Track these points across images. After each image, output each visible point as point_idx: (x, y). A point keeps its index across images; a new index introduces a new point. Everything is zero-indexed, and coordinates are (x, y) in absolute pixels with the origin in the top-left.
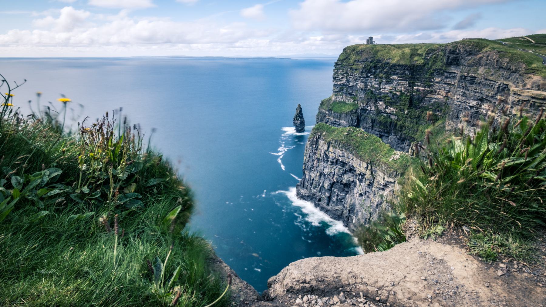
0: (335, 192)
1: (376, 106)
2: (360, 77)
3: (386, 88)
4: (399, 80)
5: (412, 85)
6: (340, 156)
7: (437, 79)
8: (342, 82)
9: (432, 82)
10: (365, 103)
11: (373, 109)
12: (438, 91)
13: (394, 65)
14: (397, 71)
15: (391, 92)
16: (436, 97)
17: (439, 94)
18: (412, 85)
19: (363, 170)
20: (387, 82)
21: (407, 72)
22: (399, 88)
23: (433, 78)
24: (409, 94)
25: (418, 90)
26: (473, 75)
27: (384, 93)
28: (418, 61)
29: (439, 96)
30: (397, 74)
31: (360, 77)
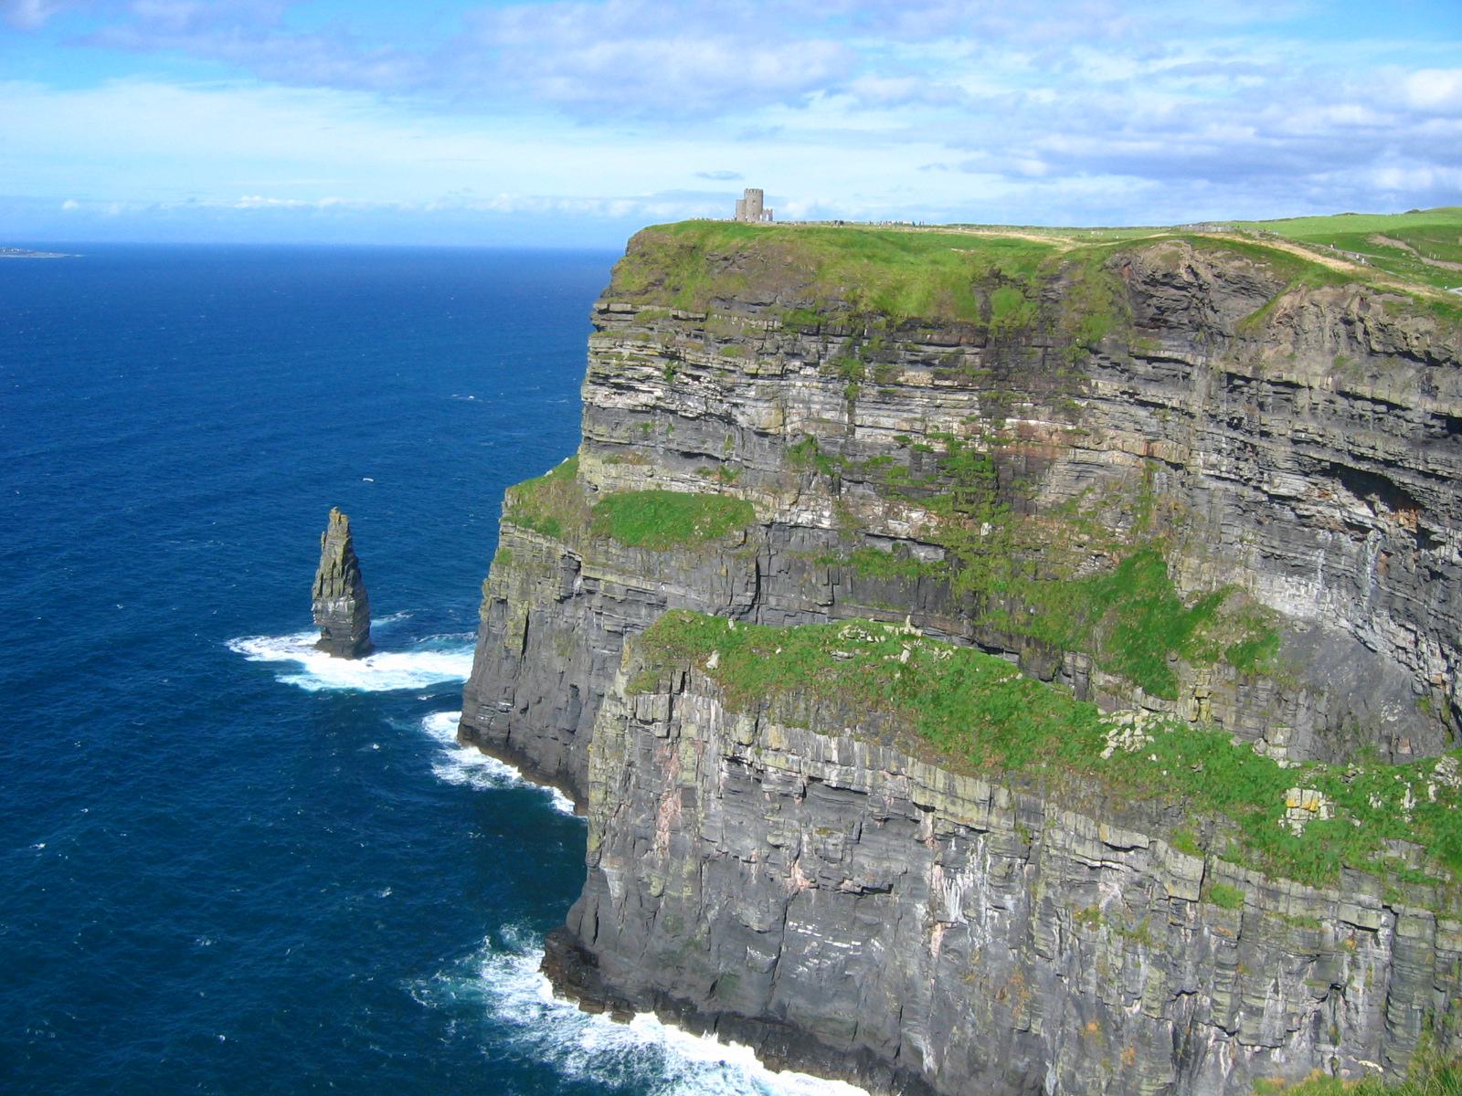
0: (805, 940)
1: (841, 511)
2: (754, 376)
3: (879, 427)
4: (936, 388)
5: (996, 410)
6: (828, 762)
7: (1106, 386)
8: (643, 398)
9: (1081, 396)
10: (788, 498)
11: (826, 524)
12: (1112, 433)
13: (911, 325)
14: (931, 350)
16: (1103, 458)
17: (1114, 448)
18: (996, 410)
19: (976, 816)
20: (885, 398)
21: (972, 357)
22: (940, 419)
23: (1087, 382)
24: (982, 449)
25: (1024, 434)
26: (1286, 377)
27: (872, 447)
28: (1008, 308)
29: (1116, 457)
30: (927, 363)
31: (754, 376)
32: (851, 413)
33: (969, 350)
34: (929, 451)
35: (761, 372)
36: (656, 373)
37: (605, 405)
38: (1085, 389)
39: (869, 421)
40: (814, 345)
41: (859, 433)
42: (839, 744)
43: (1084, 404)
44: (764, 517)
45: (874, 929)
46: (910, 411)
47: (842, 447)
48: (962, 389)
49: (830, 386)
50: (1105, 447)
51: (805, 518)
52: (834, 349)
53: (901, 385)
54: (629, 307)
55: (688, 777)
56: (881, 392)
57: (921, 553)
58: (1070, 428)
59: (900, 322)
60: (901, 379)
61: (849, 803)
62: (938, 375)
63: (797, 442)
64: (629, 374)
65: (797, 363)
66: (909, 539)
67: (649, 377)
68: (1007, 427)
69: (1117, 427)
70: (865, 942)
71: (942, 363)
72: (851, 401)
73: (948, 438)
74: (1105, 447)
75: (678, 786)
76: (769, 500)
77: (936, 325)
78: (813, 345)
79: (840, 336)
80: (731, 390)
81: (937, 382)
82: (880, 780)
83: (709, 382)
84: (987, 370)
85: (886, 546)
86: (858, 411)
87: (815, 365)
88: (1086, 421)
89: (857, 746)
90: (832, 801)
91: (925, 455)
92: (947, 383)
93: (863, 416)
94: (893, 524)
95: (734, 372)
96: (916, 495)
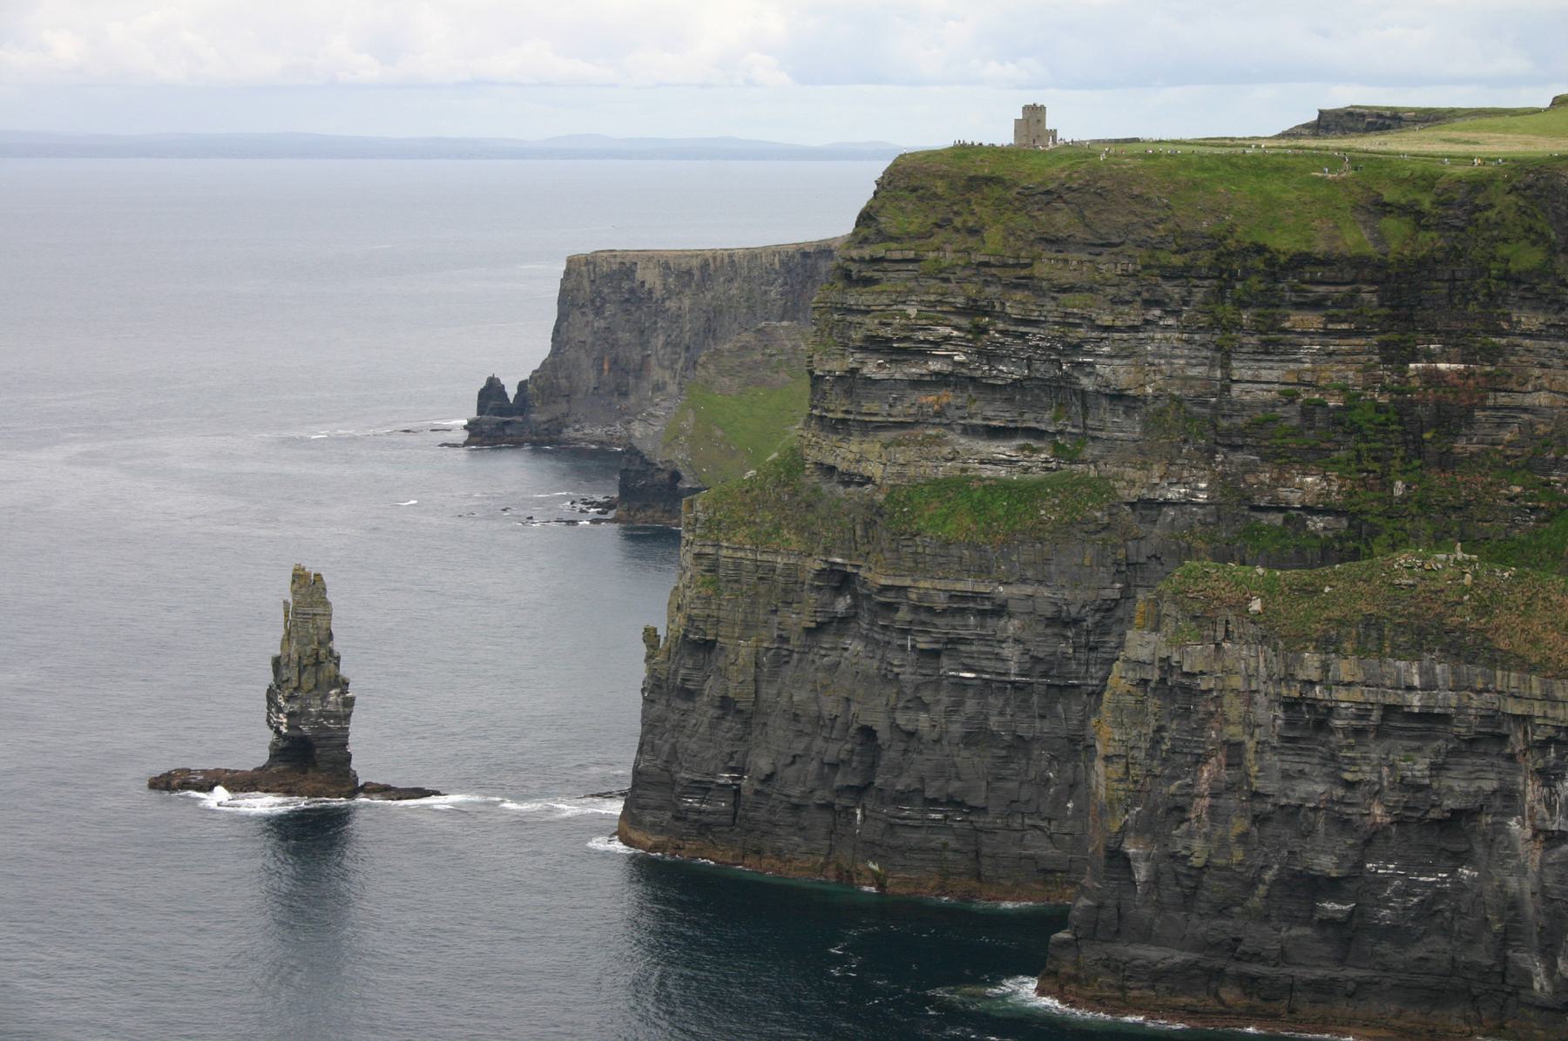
0: (1384, 881)
3: (1258, 381)
4: (1327, 333)
5: (1396, 354)
7: (1530, 320)
8: (934, 366)
9: (1500, 333)
10: (1157, 470)
12: (1537, 372)
14: (1322, 289)
15: (1291, 398)
16: (1528, 400)
17: (1536, 390)
20: (1268, 349)
21: (1368, 295)
24: (1381, 400)
25: (1433, 378)
30: (1317, 305)
32: (1225, 366)
33: (1365, 288)
34: (1323, 405)
35: (1118, 323)
36: (955, 333)
37: (878, 377)
38: (1505, 326)
39: (1248, 375)
40: (1177, 290)
41: (1236, 390)
42: (1420, 668)
43: (1504, 341)
44: (1133, 494)
45: (1461, 858)
46: (1296, 361)
47: (1214, 407)
48: (1357, 333)
49: (1197, 337)
50: (1530, 387)
51: (1174, 493)
52: (1199, 295)
53: (1286, 331)
54: (911, 255)
55: (1234, 732)
56: (1264, 341)
57: (1317, 523)
58: (1488, 369)
59: (1282, 259)
60: (1287, 325)
61: (1429, 729)
62: (1332, 319)
63: (1159, 405)
64: (921, 336)
65: (1157, 312)
66: (1304, 508)
67: (947, 338)
68: (1411, 373)
69: (1543, 366)
70: (1453, 872)
71: (1335, 305)
72: (1225, 355)
73: (1343, 389)
74: (1530, 387)
75: (1224, 743)
76: (1130, 473)
77: (1325, 262)
78: (1173, 290)
79: (1206, 278)
80: (1079, 346)
81: (1330, 326)
82: (1465, 700)
83: (1041, 339)
84: (1384, 311)
85: (1277, 519)
86: (1234, 364)
87: (1176, 313)
88: (1506, 361)
89: (1438, 668)
90: (1413, 729)
91: (1318, 410)
92: (1345, 326)
93: (1240, 370)
94: (1283, 492)
95: (1079, 325)
96: (1313, 457)
